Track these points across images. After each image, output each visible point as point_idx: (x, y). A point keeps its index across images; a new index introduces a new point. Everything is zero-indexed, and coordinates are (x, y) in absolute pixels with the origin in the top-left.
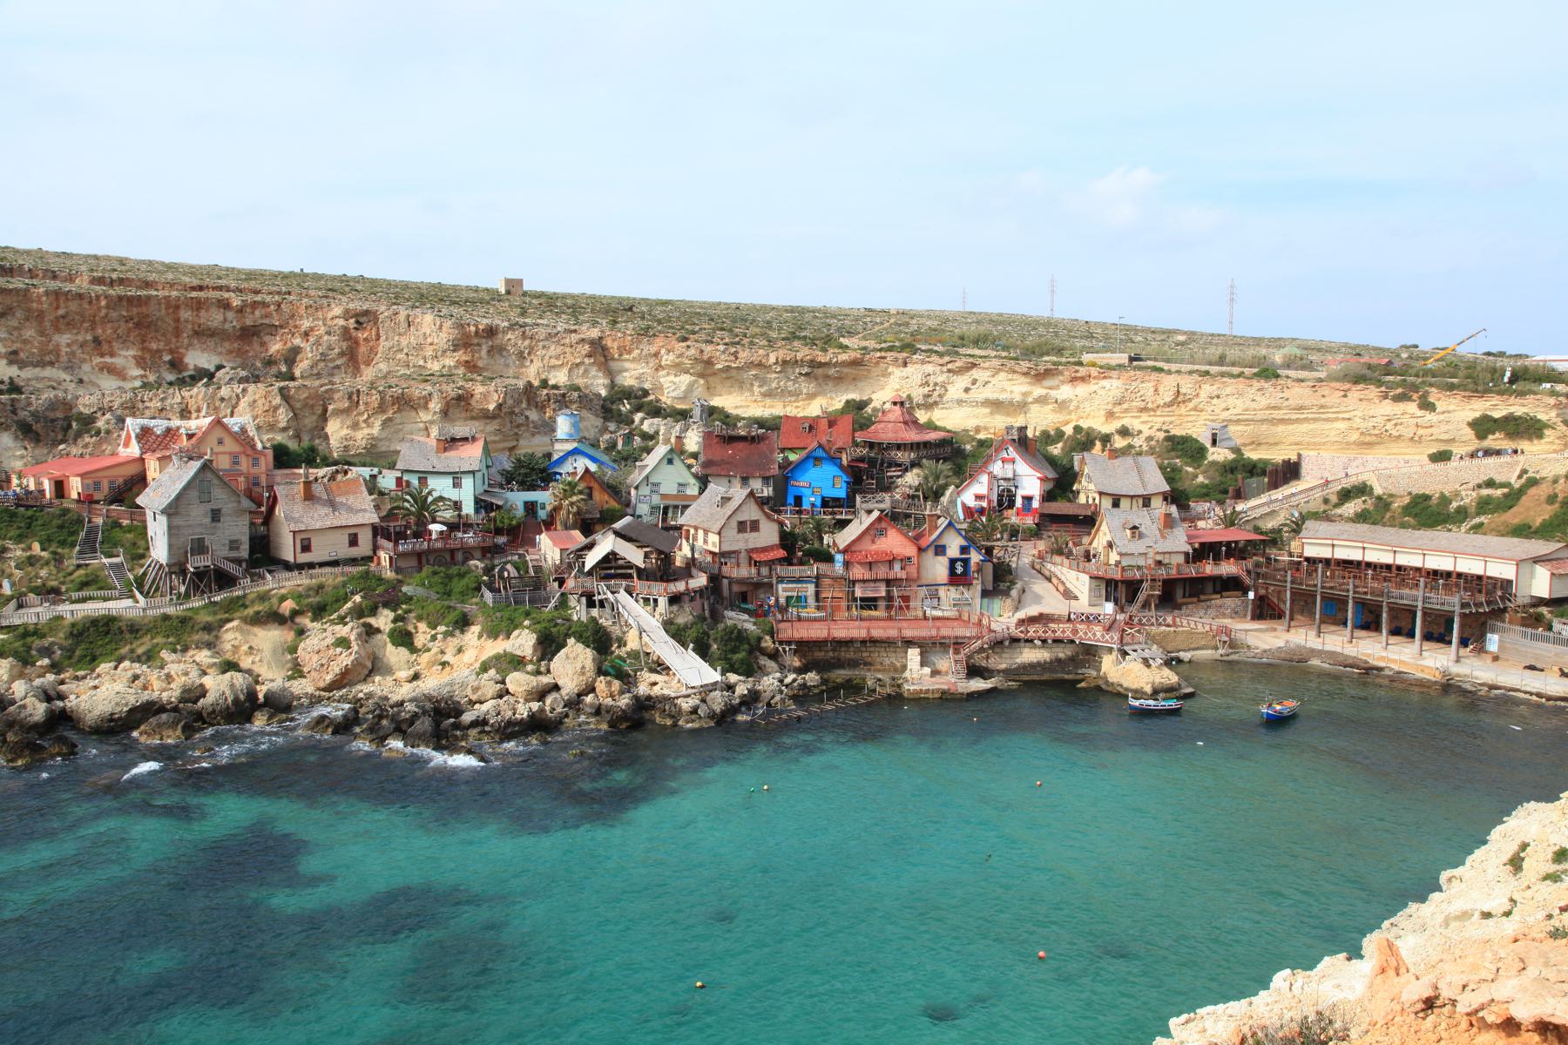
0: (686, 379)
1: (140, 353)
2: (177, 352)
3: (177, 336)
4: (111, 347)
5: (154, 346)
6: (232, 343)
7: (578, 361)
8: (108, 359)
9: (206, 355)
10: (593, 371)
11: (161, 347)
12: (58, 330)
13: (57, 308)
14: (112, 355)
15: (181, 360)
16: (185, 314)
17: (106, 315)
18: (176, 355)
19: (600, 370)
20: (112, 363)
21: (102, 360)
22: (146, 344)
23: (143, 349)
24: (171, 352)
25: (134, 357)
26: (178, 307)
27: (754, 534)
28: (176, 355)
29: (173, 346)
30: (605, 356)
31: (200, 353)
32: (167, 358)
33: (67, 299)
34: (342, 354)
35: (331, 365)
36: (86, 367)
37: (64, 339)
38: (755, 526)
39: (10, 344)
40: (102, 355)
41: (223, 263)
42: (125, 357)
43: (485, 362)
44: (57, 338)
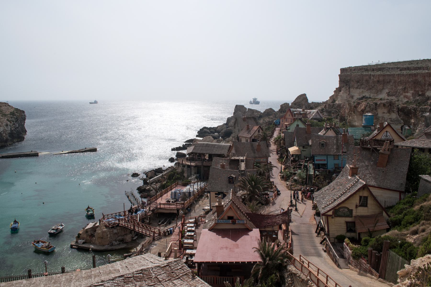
3: (425, 86)
4: (408, 90)
5: (417, 89)
8: (406, 94)
11: (419, 90)
12: (399, 86)
13: (399, 79)
14: (407, 93)
15: (425, 93)
16: (427, 78)
17: (408, 80)
18: (423, 92)
20: (407, 95)
21: (405, 94)
22: (416, 89)
23: (415, 91)
24: (422, 91)
25: (412, 93)
26: (425, 76)
28: (423, 92)
33: (401, 76)
36: (402, 96)
40: (405, 93)
41: (353, 66)
42: (410, 93)
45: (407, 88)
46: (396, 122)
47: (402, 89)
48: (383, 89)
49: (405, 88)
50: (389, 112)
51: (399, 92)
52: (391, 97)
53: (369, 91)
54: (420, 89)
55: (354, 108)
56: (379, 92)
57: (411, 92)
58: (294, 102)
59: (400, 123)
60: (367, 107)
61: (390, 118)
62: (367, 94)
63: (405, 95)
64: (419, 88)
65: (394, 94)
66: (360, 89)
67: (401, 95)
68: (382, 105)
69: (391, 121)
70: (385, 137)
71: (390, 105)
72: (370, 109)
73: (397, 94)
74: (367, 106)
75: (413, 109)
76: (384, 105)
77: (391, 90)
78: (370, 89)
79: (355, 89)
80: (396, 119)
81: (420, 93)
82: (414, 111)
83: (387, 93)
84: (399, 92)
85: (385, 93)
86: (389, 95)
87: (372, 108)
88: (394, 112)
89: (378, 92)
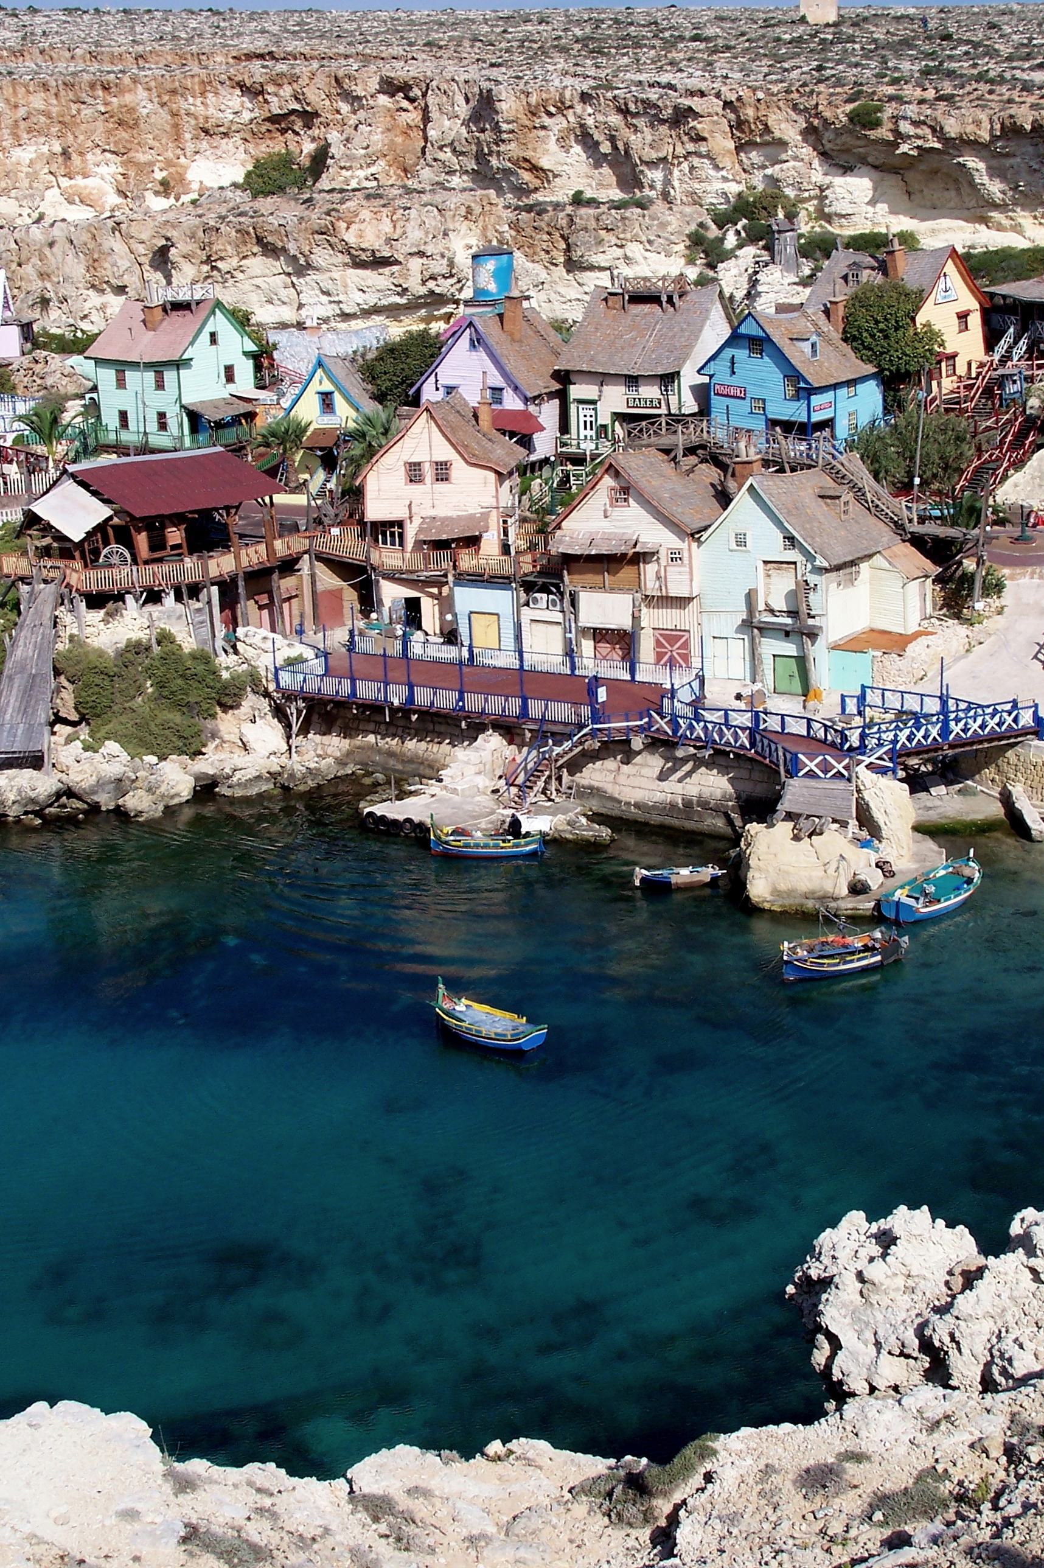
1: (121, 170)
8: (79, 181)
14: (86, 176)
15: (181, 179)
20: (86, 187)
27: (441, 486)
32: (159, 175)
37: (25, 154)
38: (442, 472)
44: (18, 154)
45: (81, 154)
57: (103, 170)
60: (412, 223)
63: (76, 185)
72: (427, 233)
84: (33, 177)
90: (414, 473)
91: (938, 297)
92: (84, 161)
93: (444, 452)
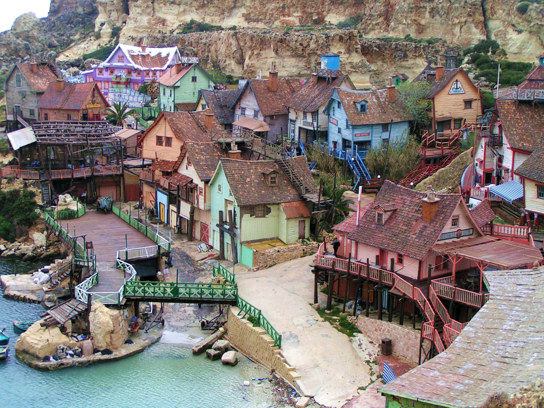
0: (524, 36)
1: (301, 15)
2: (321, 14)
5: (309, 10)
6: (351, 9)
7: (463, 20)
8: (287, 18)
9: (338, 16)
10: (474, 30)
11: (313, 11)
14: (289, 16)
19: (476, 27)
21: (284, 18)
22: (306, 9)
23: (304, 12)
24: (318, 14)
29: (320, 10)
30: (484, 15)
31: (335, 15)
34: (380, 16)
35: (374, 23)
38: (169, 141)
39: (249, 9)
40: (284, 16)
43: (427, 21)
45: (289, 8)
46: (361, 69)
47: (277, 9)
48: (235, 7)
49: (284, 5)
50: (349, 51)
51: (272, 15)
52: (255, 23)
53: (201, 11)
54: (314, 9)
55: (279, 44)
56: (226, 13)
57: (296, 14)
58: (14, 32)
59: (370, 71)
60: (312, 41)
61: (350, 63)
62: (197, 18)
64: (313, 7)
65: (261, 17)
66: (179, 5)
67: (275, 20)
68: (338, 38)
69: (351, 67)
70: (454, 90)
71: (350, 37)
72: (318, 46)
73: (268, 18)
74: (311, 40)
75: (376, 46)
76: (341, 39)
77: (252, 10)
78: (203, 6)
79: (168, 4)
80: (360, 64)
81: (315, 18)
82: (377, 50)
83: (243, 15)
84: (272, 15)
85: (240, 14)
86: (247, 18)
87: (322, 44)
88: (357, 52)
89: (223, 14)
90: (159, 140)
91: (451, 90)
92: (289, 11)
93: (170, 134)
